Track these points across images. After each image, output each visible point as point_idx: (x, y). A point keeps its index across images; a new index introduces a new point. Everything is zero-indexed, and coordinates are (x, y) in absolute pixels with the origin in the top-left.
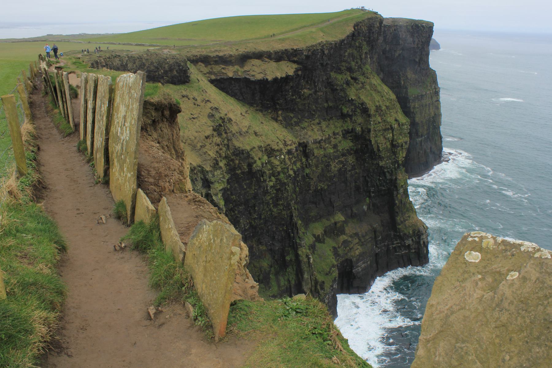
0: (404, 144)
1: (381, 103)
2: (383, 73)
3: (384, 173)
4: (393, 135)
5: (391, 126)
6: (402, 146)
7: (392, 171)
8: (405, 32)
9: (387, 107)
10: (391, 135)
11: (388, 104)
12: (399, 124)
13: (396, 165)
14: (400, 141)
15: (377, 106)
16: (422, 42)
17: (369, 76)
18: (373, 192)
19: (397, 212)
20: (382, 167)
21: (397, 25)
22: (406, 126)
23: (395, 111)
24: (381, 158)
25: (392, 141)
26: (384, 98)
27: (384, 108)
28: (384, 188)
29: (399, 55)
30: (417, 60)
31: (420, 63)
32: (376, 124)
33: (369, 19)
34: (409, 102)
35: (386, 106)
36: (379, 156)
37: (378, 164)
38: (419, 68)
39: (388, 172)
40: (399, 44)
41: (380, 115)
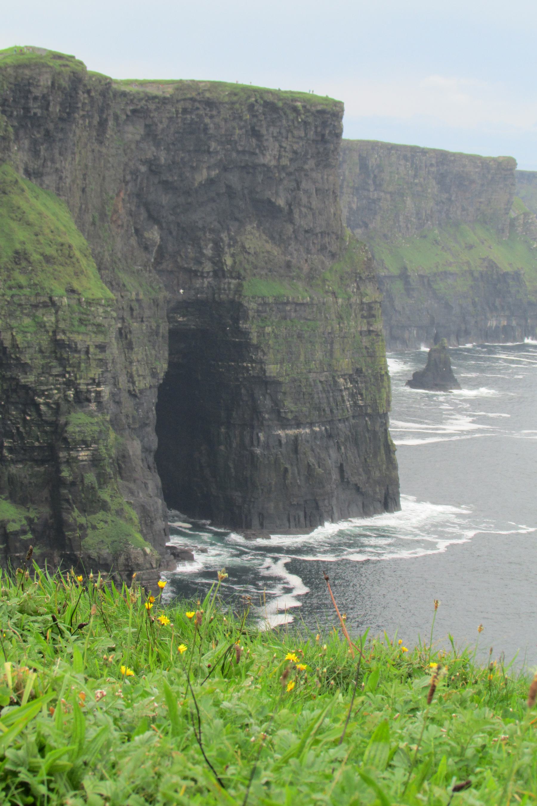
0: (92, 350)
1: (29, 247)
2: (161, 228)
3: (37, 406)
4: (57, 321)
5: (51, 298)
6: (87, 352)
7: (57, 404)
8: (226, 120)
9: (48, 259)
10: (53, 319)
11: (50, 251)
12: (79, 300)
13: (71, 393)
14: (78, 338)
15: (17, 252)
16: (295, 152)
17: (8, 189)
18: (11, 450)
19: (67, 501)
20: (26, 387)
21: (193, 100)
22: (101, 310)
23: (70, 270)
24: (25, 368)
25: (54, 332)
26: (40, 237)
27: (35, 257)
28: (37, 444)
29: (211, 182)
30: (281, 202)
31: (291, 212)
32: (10, 288)
33: (18, 67)
34: (246, 318)
35: (42, 254)
36: (18, 359)
37: (18, 380)
38: (290, 228)
39: (47, 404)
40: (209, 152)
41: (23, 271)
